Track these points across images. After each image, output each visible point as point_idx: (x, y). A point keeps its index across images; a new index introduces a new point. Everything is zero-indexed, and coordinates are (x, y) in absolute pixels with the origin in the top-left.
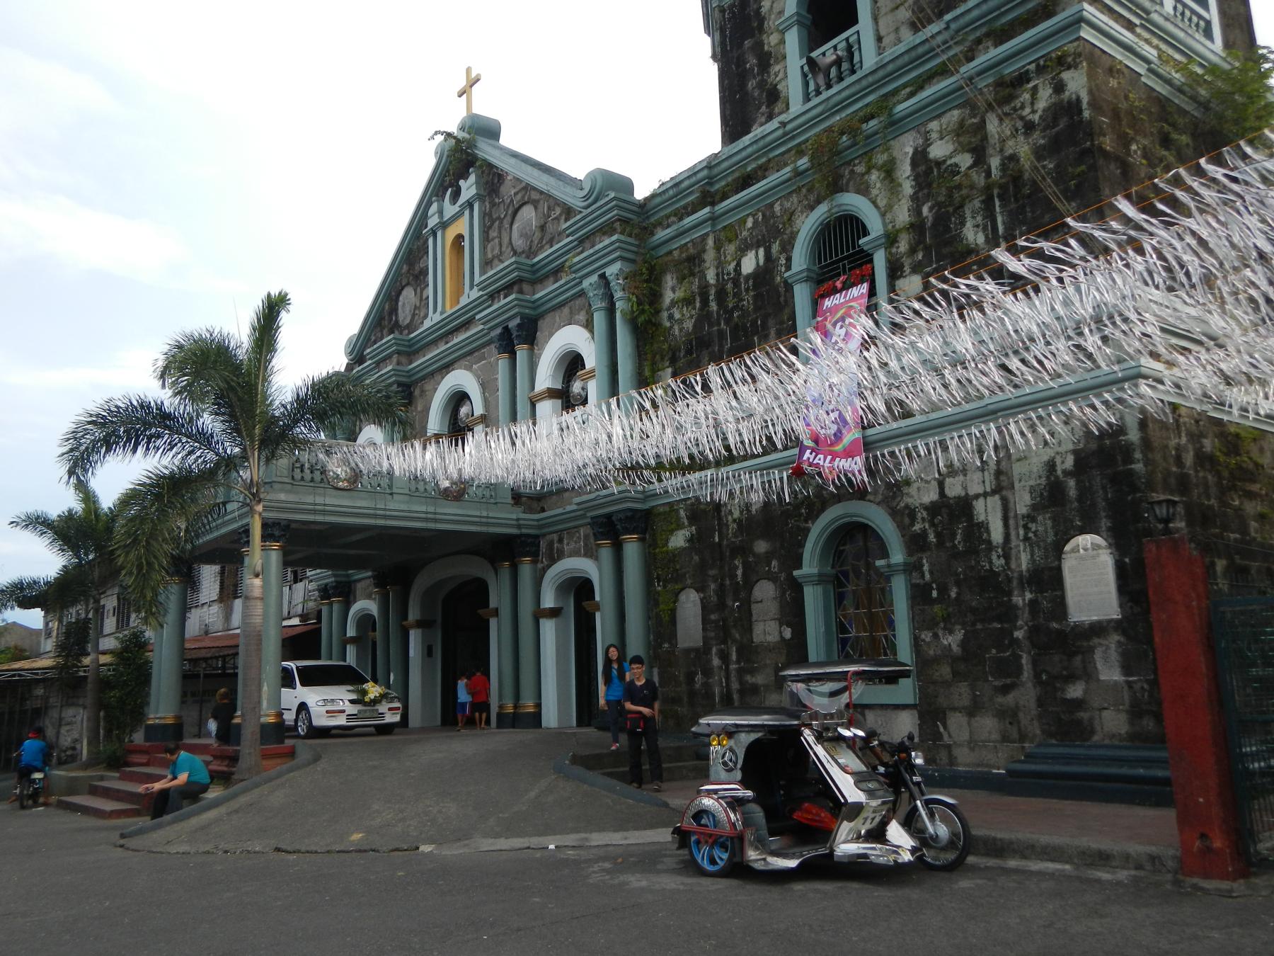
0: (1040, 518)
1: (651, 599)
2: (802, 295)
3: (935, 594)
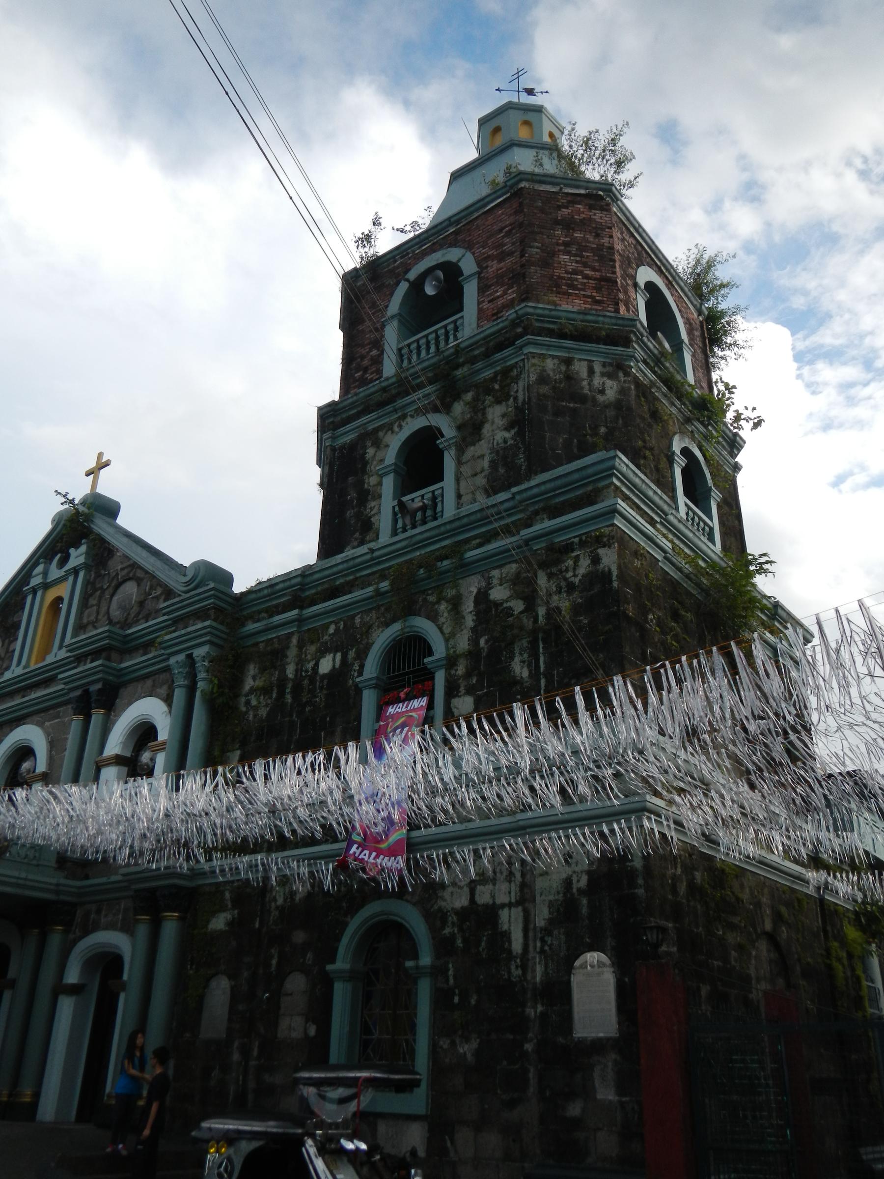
0: (556, 932)
1: (181, 981)
2: (369, 699)
3: (456, 1000)
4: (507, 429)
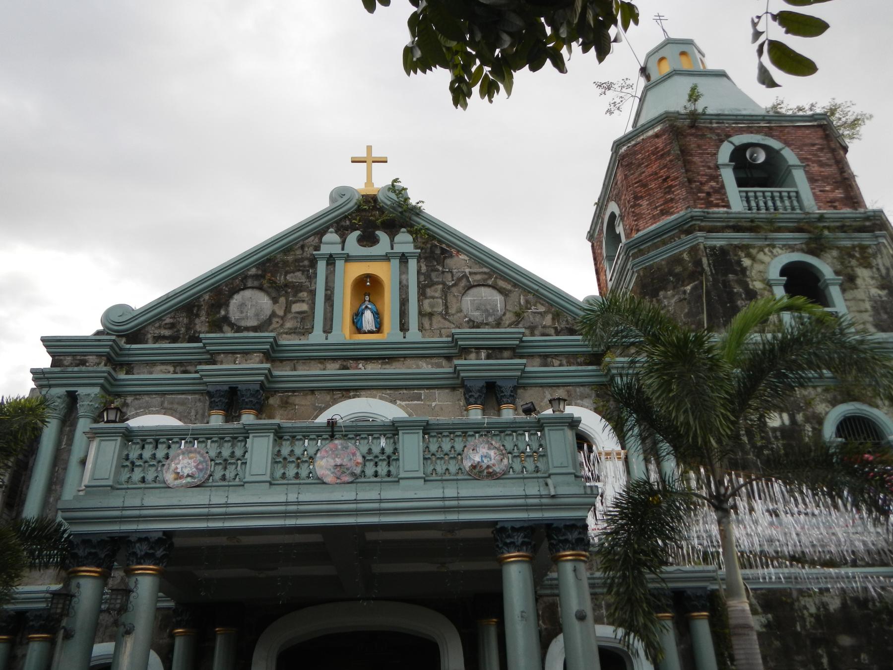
4: (882, 287)
